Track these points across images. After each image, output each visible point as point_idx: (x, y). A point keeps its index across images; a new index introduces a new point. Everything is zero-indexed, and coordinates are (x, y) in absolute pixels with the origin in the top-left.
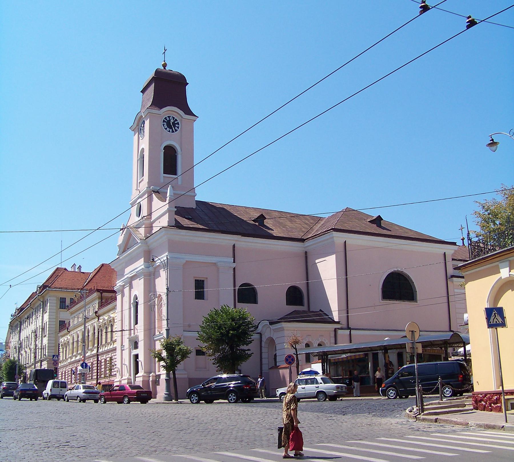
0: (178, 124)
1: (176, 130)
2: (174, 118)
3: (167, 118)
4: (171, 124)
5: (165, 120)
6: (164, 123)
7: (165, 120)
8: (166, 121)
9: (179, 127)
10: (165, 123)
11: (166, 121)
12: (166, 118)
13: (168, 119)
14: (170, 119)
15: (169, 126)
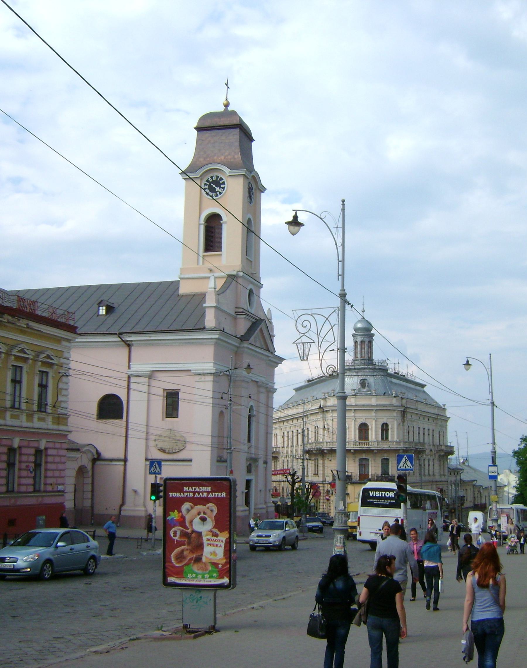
0: (224, 183)
1: (220, 193)
2: (218, 177)
3: (209, 180)
4: (214, 186)
5: (207, 183)
6: (206, 186)
7: (207, 183)
8: (208, 184)
9: (225, 187)
10: (207, 186)
11: (208, 184)
12: (208, 181)
13: (210, 181)
14: (214, 179)
15: (213, 190)
